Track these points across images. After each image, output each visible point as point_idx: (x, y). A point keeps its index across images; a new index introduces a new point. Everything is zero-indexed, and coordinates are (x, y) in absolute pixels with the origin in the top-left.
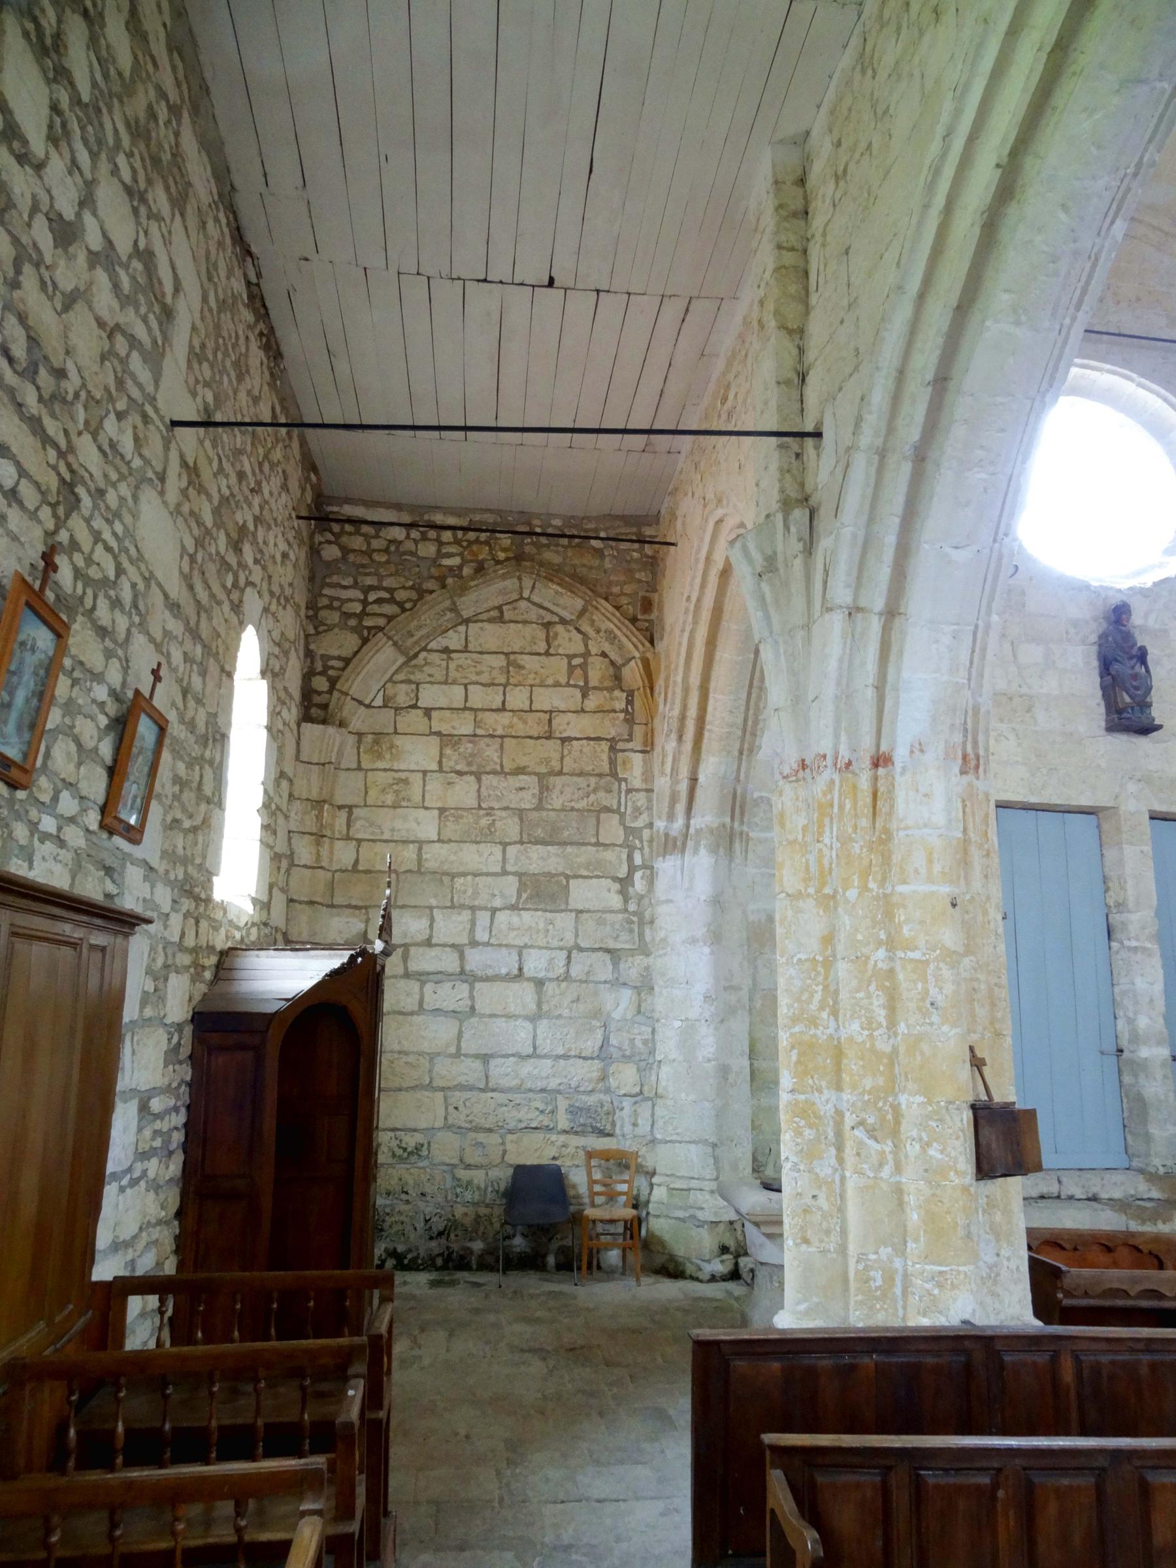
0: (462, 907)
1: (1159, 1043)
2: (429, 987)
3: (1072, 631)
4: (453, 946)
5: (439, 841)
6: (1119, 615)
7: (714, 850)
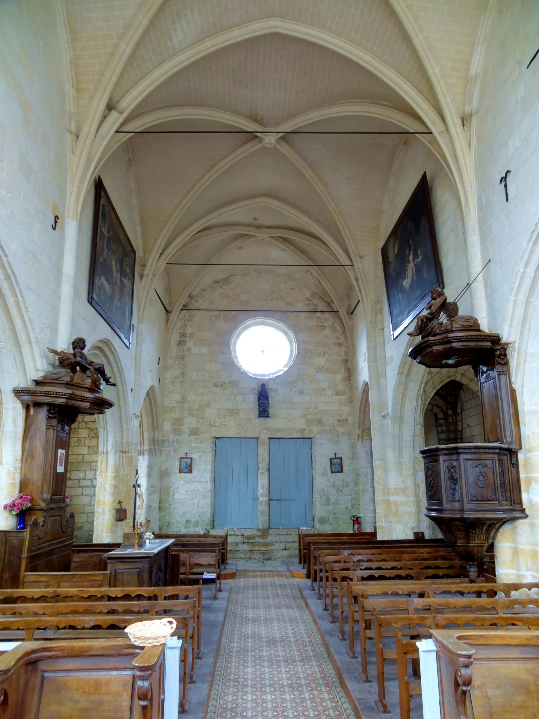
0: (93, 470)
1: (265, 496)
2: (84, 489)
3: (251, 391)
4: (90, 479)
5: (88, 454)
6: (263, 386)
7: (149, 454)
